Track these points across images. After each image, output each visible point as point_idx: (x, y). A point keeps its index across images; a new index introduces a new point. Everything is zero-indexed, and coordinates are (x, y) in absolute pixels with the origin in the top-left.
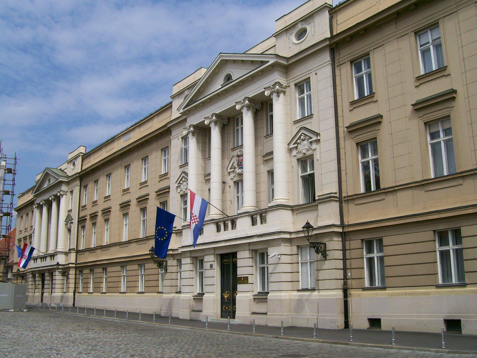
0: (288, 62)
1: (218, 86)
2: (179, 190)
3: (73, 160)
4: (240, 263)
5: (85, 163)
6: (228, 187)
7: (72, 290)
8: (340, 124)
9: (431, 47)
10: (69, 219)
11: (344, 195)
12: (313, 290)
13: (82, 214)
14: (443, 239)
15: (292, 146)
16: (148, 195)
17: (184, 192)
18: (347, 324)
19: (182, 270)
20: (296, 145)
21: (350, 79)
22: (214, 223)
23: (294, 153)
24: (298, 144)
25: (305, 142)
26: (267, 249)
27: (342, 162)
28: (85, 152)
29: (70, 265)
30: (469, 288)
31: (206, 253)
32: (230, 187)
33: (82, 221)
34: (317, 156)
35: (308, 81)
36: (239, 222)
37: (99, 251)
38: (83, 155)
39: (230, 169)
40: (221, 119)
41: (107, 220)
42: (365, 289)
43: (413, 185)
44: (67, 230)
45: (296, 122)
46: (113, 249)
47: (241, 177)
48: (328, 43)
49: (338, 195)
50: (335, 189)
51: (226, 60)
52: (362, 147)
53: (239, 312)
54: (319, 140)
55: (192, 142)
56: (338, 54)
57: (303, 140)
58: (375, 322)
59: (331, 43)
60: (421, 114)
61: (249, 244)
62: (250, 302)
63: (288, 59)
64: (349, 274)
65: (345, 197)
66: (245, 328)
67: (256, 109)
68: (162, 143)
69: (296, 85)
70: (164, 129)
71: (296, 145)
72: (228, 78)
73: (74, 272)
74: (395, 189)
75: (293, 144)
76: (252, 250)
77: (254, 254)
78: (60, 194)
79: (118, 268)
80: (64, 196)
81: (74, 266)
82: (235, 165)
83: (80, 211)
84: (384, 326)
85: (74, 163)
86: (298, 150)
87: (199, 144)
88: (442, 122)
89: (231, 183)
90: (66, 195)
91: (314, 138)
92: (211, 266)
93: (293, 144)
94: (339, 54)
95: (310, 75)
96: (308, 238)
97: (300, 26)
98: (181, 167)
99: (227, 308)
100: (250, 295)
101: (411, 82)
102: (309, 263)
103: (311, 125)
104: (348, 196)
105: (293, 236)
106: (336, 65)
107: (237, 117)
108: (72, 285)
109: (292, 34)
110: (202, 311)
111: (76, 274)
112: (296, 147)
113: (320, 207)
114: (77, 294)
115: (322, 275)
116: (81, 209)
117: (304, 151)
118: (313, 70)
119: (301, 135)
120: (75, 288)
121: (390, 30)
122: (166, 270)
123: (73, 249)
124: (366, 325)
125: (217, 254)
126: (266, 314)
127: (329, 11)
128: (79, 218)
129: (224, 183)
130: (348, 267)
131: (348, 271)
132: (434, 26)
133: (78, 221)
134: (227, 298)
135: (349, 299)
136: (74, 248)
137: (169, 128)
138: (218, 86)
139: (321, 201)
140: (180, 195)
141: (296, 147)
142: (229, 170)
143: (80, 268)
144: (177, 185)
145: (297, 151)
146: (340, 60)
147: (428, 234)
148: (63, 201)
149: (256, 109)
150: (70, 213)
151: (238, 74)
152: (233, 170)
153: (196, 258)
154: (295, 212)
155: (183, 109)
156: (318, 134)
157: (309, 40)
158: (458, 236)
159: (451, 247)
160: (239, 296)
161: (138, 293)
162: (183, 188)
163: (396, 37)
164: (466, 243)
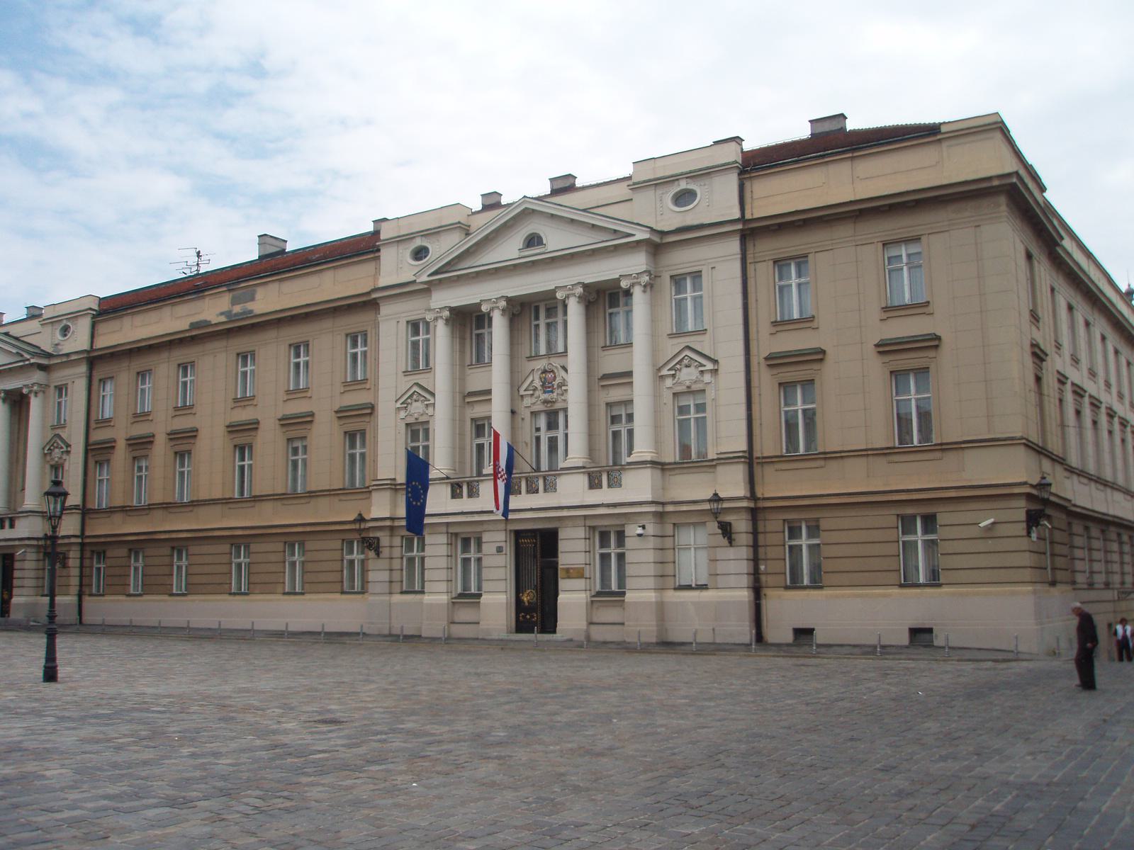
0: (661, 238)
1: (510, 249)
2: (403, 414)
3: (65, 322)
4: (562, 546)
5: (102, 328)
6: (520, 420)
7: (74, 590)
8: (753, 350)
9: (905, 269)
10: (55, 444)
11: (757, 454)
12: (703, 587)
13: (98, 436)
14: (907, 524)
15: (665, 372)
16: (312, 415)
17: (416, 419)
18: (760, 638)
19: (426, 554)
20: (673, 372)
21: (772, 289)
23: (669, 382)
24: (676, 371)
25: (692, 370)
26: (623, 525)
27: (755, 407)
28: (96, 308)
29: (73, 540)
30: (945, 589)
31: (485, 527)
32: (523, 419)
33: (97, 453)
34: (710, 394)
35: (697, 276)
36: (564, 483)
37: (158, 514)
38: (95, 313)
39: (525, 390)
40: (512, 305)
41: (181, 455)
42: (787, 588)
43: (869, 452)
44: (48, 467)
45: (671, 336)
46: (202, 511)
47: (549, 405)
48: (740, 226)
49: (747, 455)
50: (743, 446)
51: (534, 211)
52: (786, 386)
53: (562, 623)
54: (717, 370)
55: (441, 336)
56: (752, 244)
58: (803, 634)
59: (746, 227)
60: (887, 358)
61: (585, 517)
62: (587, 605)
63: (663, 233)
64: (762, 567)
65: (758, 458)
66: (588, 645)
67: (589, 302)
68: (354, 322)
69: (671, 277)
70: (364, 299)
71: (673, 372)
72: (533, 241)
73: (78, 555)
74: (843, 454)
75: (669, 370)
76: (589, 527)
77: (591, 533)
78: (30, 392)
79: (225, 548)
80: (40, 395)
81: (79, 540)
82: (538, 383)
83: (91, 431)
84: (820, 637)
85: (65, 330)
86: (676, 380)
87: (455, 339)
88: (915, 373)
89: (527, 415)
90: (44, 392)
91: (710, 366)
92: (499, 550)
93: (669, 370)
94: (754, 245)
95: (703, 267)
96: (715, 514)
97: (683, 185)
98: (406, 373)
99: (528, 617)
100: (582, 597)
101: (874, 313)
102: (693, 549)
103: (704, 345)
104: (764, 458)
105: (670, 508)
106: (749, 261)
107: (537, 304)
108: (75, 581)
109: (667, 192)
110: (478, 623)
111: (82, 558)
113: (719, 469)
114: (86, 599)
115: (721, 567)
116: (93, 425)
117: (688, 383)
118: (709, 261)
119: (683, 358)
120: (81, 585)
121: (843, 232)
122: (378, 554)
123: (76, 507)
124: (789, 638)
125: (510, 531)
126: (623, 624)
127: (739, 175)
128: (87, 444)
129: (513, 412)
130: (761, 556)
131: (761, 562)
132: (916, 239)
133: (87, 452)
134: (528, 601)
135: (763, 602)
136: (78, 506)
137: (375, 299)
138: (510, 249)
139: (723, 461)
140: (407, 424)
141: (674, 376)
142: (522, 392)
143: (94, 549)
144: (398, 405)
146: (756, 255)
147: (888, 517)
148: (35, 404)
149: (589, 302)
150: (59, 431)
151: (557, 240)
152: (531, 392)
153: (456, 535)
154: (668, 473)
156: (715, 362)
157: (698, 213)
158: (930, 522)
159: (919, 537)
160: (562, 598)
161: (284, 594)
162: (412, 412)
163: (854, 244)
164: (942, 533)
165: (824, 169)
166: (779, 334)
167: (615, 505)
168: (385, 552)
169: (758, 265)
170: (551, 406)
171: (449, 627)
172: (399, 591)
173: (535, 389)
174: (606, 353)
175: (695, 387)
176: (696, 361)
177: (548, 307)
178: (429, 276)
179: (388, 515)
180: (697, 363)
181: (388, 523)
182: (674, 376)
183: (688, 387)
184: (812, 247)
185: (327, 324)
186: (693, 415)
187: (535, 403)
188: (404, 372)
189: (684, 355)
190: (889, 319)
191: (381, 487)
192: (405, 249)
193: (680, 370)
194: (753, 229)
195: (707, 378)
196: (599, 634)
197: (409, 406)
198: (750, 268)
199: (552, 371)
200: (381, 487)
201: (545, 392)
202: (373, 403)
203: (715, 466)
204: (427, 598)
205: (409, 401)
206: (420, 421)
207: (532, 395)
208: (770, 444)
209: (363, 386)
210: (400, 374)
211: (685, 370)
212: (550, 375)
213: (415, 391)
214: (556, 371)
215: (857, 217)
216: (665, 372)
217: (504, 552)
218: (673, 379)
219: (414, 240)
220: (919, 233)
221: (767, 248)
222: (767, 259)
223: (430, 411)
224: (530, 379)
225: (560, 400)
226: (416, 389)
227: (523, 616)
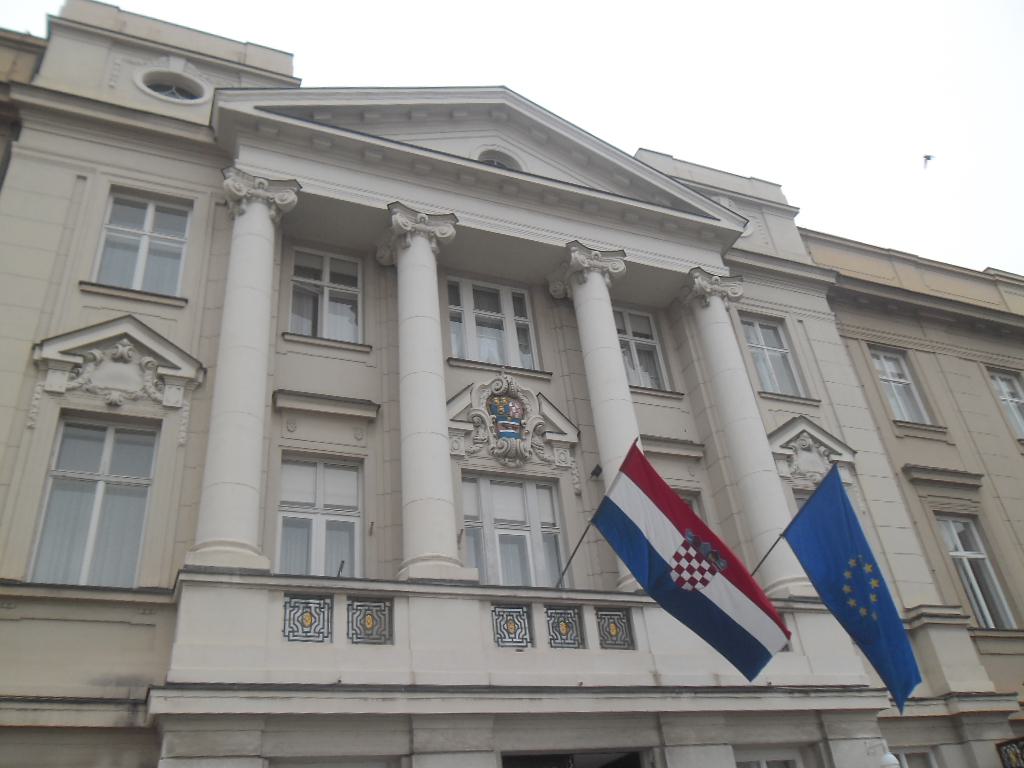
2: (58, 381)
22: (482, 599)
47: (512, 464)
48: (833, 280)
57: (808, 449)
95: (787, 315)
119: (798, 437)
137: (15, 106)
144: (51, 352)
152: (470, 427)
155: (257, 108)
156: (855, 452)
162: (97, 383)
167: (805, 691)
170: (517, 467)
173: (479, 423)
176: (822, 444)
178: (257, 108)
180: (822, 449)
182: (789, 458)
187: (474, 452)
188: (81, 283)
189: (801, 430)
192: (131, 63)
197: (92, 365)
201: (499, 436)
205: (97, 353)
206: (123, 413)
207: (467, 433)
211: (804, 455)
214: (525, 400)
218: (790, 466)
219: (164, 59)
223: (173, 395)
225: (535, 458)
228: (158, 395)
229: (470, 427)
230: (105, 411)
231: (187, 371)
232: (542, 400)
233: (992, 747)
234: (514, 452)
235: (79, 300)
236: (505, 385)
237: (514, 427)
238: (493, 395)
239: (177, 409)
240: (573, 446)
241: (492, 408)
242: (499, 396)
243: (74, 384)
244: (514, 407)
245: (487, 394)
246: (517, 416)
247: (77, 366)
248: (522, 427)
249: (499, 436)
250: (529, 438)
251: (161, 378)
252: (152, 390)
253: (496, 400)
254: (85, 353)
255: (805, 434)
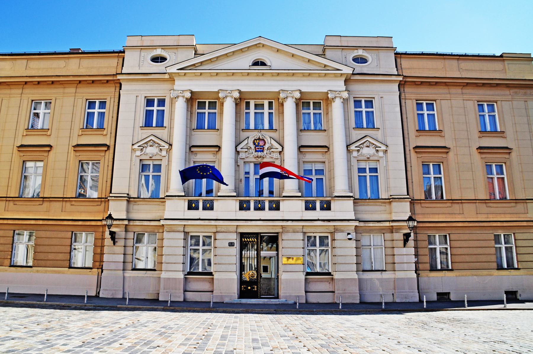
20: (359, 149)
23: (355, 154)
71: (359, 149)
82: (253, 147)
86: (360, 153)
91: (383, 148)
112: (358, 151)
113: (394, 204)
117: (368, 156)
119: (365, 142)
145: (359, 154)
152: (247, 150)
156: (387, 146)
163: (462, 99)
165: (443, 61)
166: (421, 137)
168: (121, 243)
169: (407, 101)
171: (184, 294)
172: (131, 269)
174: (303, 133)
175: (371, 158)
176: (374, 144)
177: (256, 103)
179: (125, 218)
181: (126, 222)
182: (358, 151)
183: (368, 158)
184: (439, 97)
185: (71, 90)
186: (368, 174)
190: (483, 138)
191: (118, 198)
193: (362, 148)
194: (405, 82)
195: (381, 154)
196: (313, 298)
197: (145, 148)
198: (403, 101)
199: (263, 140)
200: (118, 198)
202: (108, 144)
203: (390, 202)
204: (164, 275)
208: (419, 194)
209: (101, 133)
210: (138, 128)
212: (261, 143)
213: (151, 140)
215: (464, 86)
216: (353, 147)
217: (235, 246)
220: (497, 100)
221: (411, 92)
222: (412, 98)
224: (246, 142)
226: (152, 138)
227: (244, 288)
228: (160, 154)
229: (247, 150)
230: (149, 159)
231: (167, 146)
232: (271, 139)
233: (402, 234)
234: (259, 156)
235: (141, 131)
236: (258, 137)
237: (261, 149)
238: (255, 139)
239: (165, 156)
240: (280, 152)
241: (254, 144)
242: (256, 140)
243: (141, 154)
244: (261, 143)
245: (253, 139)
246: (262, 145)
247: (142, 149)
248: (264, 148)
249: (256, 151)
250: (265, 152)
251: (161, 149)
252: (159, 153)
253: (255, 141)
254: (143, 146)
255: (367, 142)
